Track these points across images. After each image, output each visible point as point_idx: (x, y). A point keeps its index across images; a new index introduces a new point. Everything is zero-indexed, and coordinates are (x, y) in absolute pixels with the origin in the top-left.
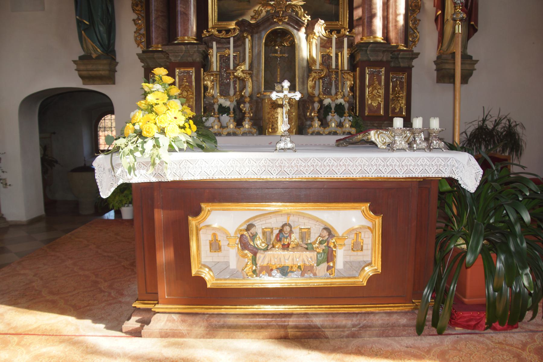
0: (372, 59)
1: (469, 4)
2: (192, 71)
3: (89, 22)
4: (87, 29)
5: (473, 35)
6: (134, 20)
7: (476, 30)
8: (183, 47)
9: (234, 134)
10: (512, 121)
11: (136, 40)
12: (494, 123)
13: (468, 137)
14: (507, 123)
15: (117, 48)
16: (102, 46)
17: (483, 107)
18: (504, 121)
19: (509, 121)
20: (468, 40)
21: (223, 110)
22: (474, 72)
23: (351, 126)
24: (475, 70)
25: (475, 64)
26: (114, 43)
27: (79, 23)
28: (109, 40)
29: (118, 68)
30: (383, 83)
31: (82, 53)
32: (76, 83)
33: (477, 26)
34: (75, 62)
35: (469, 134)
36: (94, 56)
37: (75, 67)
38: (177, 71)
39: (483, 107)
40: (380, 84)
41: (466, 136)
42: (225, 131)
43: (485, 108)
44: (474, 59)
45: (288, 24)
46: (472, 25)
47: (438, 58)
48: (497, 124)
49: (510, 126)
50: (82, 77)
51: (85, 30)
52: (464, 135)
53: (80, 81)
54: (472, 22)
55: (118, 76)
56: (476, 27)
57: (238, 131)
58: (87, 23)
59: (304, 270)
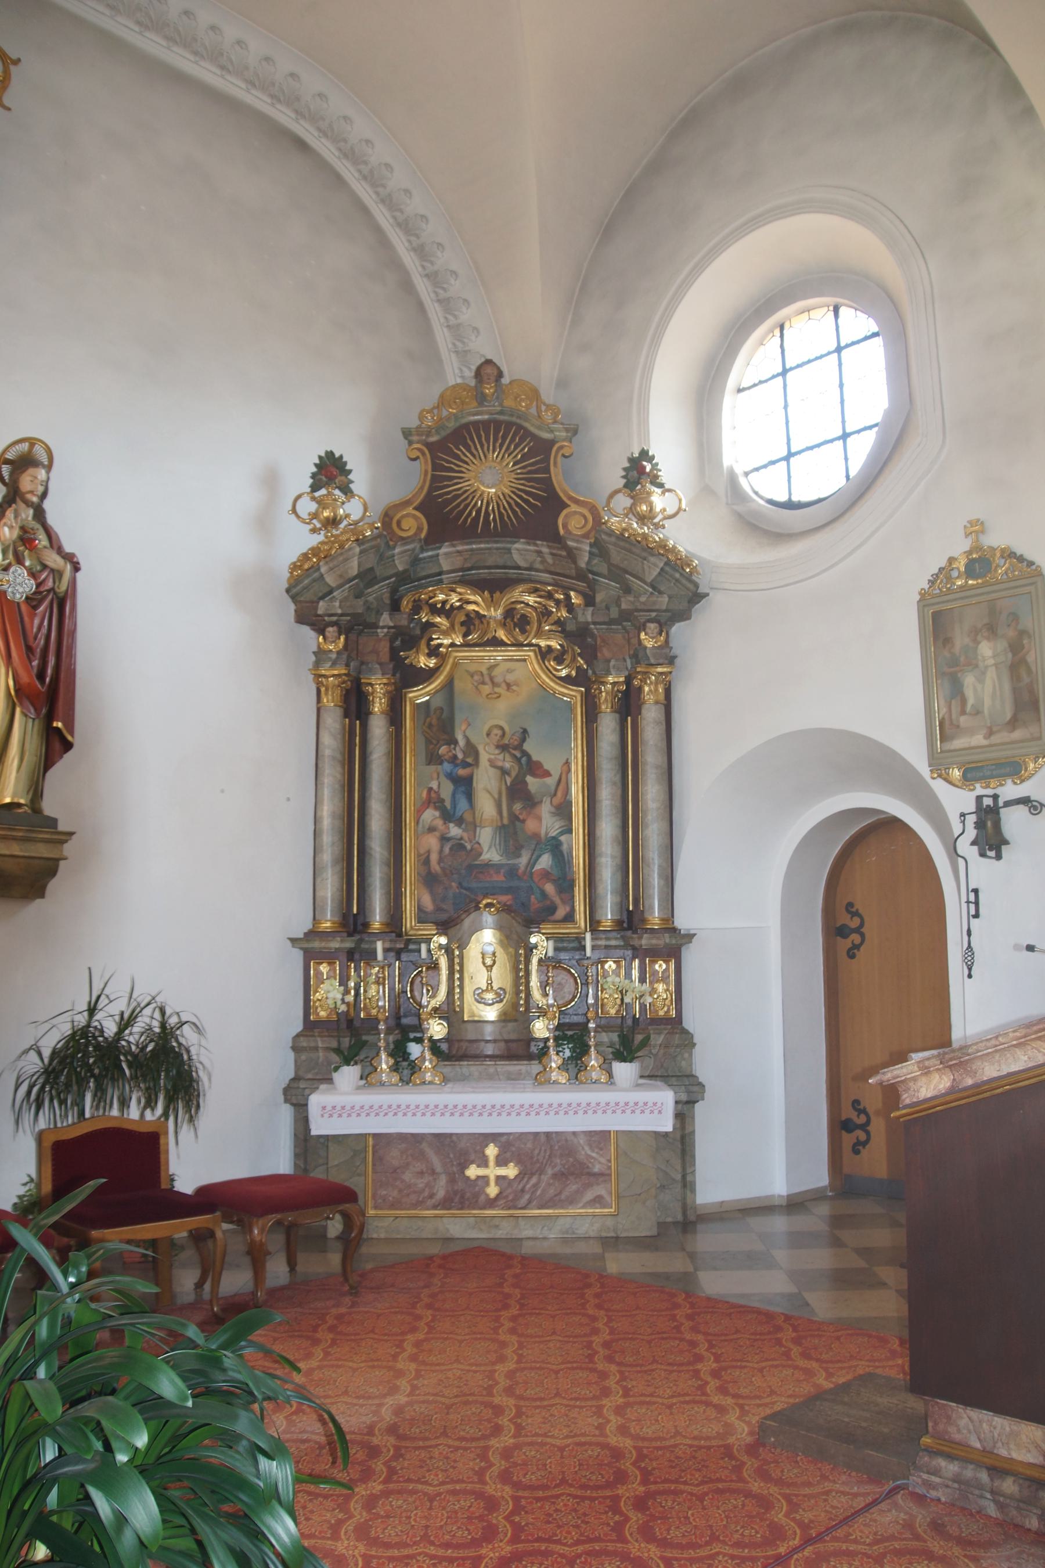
1: (49, 671)
5: (61, 757)
7: (68, 746)
10: (168, 1012)
12: (117, 1018)
13: (46, 1061)
14: (157, 1015)
17: (90, 969)
18: (147, 1011)
19: (163, 1012)
20: (46, 770)
22: (62, 863)
24: (65, 859)
25: (66, 841)
33: (73, 736)
35: (47, 1053)
39: (90, 969)
41: (37, 1060)
43: (93, 971)
44: (62, 827)
46: (57, 729)
48: (126, 1023)
49: (163, 1025)
52: (33, 1056)
54: (58, 721)
56: (70, 738)
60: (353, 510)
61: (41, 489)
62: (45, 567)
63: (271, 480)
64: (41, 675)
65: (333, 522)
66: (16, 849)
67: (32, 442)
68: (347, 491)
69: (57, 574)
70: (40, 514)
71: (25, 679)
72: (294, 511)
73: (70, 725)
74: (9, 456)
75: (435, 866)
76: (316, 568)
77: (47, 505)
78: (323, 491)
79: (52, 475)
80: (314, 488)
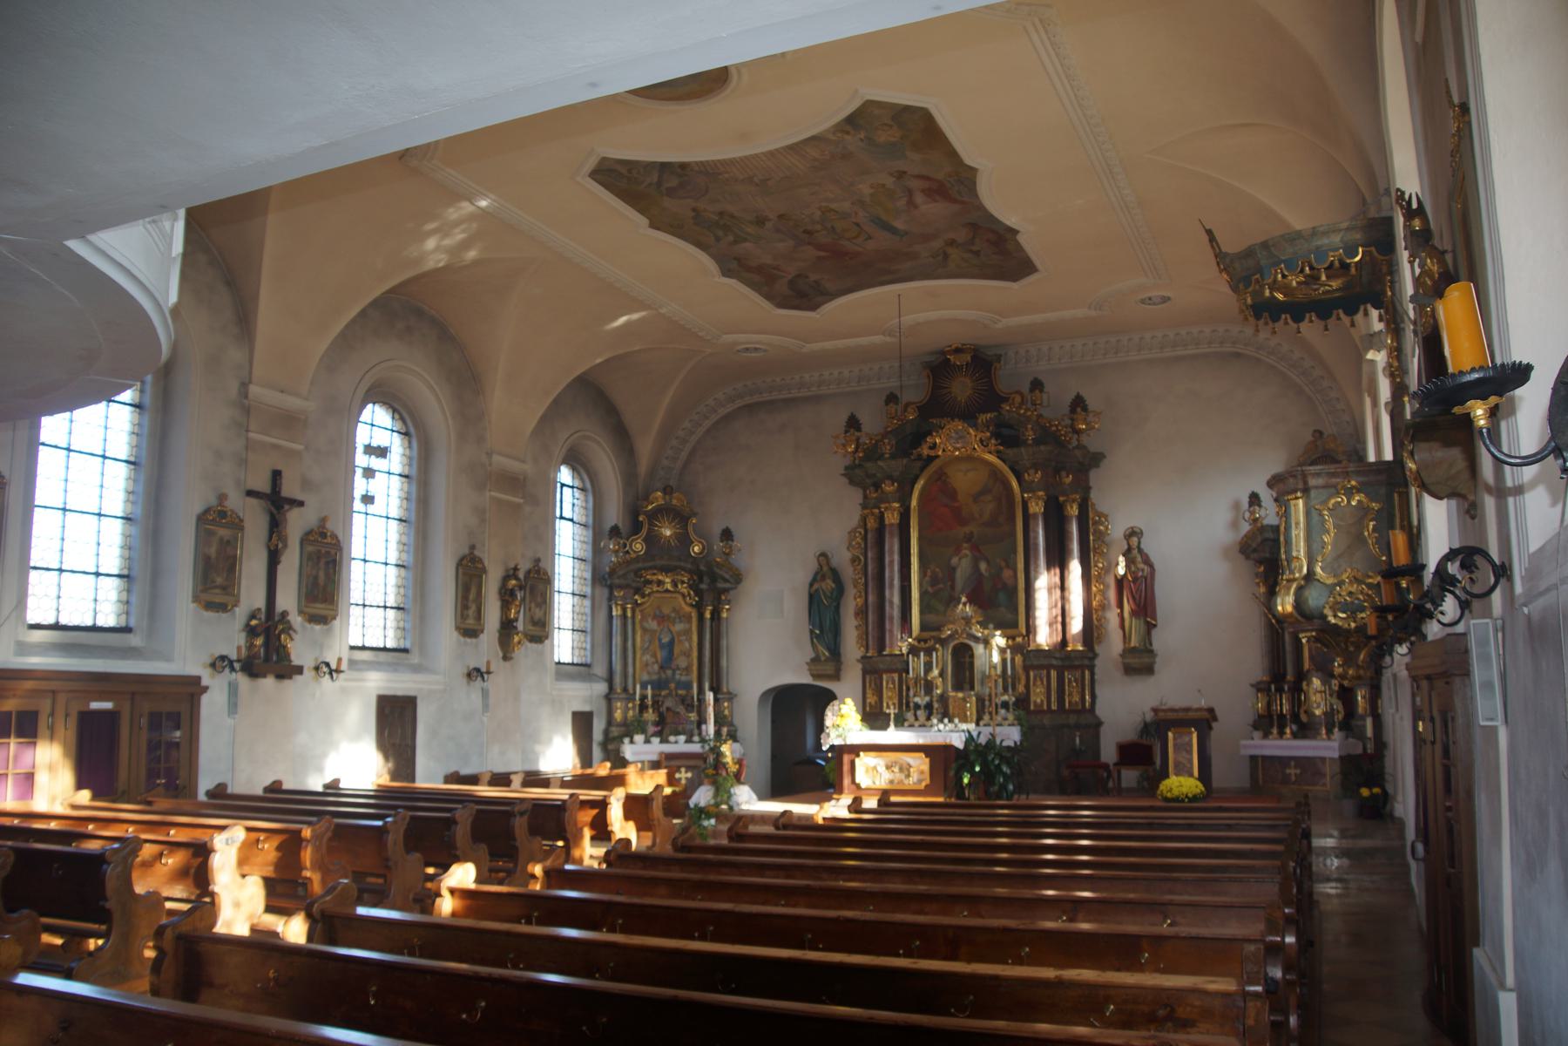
0: (1035, 663)
2: (896, 676)
3: (820, 631)
4: (818, 637)
6: (856, 627)
7: (1155, 626)
8: (888, 658)
9: (924, 726)
11: (857, 642)
15: (842, 651)
16: (829, 650)
21: (917, 707)
23: (1015, 719)
26: (839, 647)
27: (812, 632)
28: (835, 644)
29: (843, 667)
30: (1045, 683)
31: (813, 655)
32: (805, 679)
33: (1156, 620)
34: (807, 663)
36: (823, 659)
37: (806, 667)
38: (885, 677)
40: (1042, 683)
42: (917, 724)
45: (966, 638)
47: (1124, 651)
50: (813, 676)
51: (816, 638)
53: (811, 678)
55: (843, 674)
57: (926, 723)
58: (818, 632)
59: (901, 782)
60: (1263, 513)
61: (1136, 544)
62: (1138, 569)
63: (1236, 506)
64: (1138, 605)
65: (1256, 520)
66: (1137, 660)
67: (1132, 528)
68: (1260, 506)
69: (1143, 570)
70: (1140, 550)
71: (1133, 607)
72: (1244, 518)
73: (1154, 617)
74: (1127, 533)
75: (1314, 652)
76: (1246, 542)
77: (1142, 546)
78: (1252, 509)
79: (1142, 540)
80: (1250, 506)
